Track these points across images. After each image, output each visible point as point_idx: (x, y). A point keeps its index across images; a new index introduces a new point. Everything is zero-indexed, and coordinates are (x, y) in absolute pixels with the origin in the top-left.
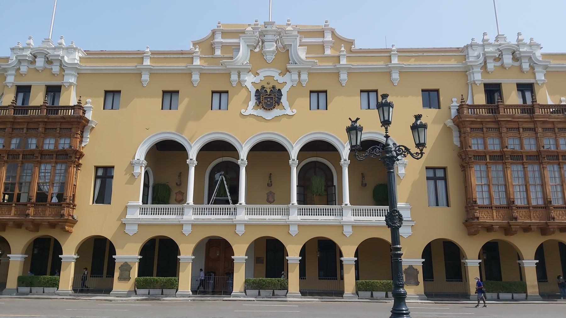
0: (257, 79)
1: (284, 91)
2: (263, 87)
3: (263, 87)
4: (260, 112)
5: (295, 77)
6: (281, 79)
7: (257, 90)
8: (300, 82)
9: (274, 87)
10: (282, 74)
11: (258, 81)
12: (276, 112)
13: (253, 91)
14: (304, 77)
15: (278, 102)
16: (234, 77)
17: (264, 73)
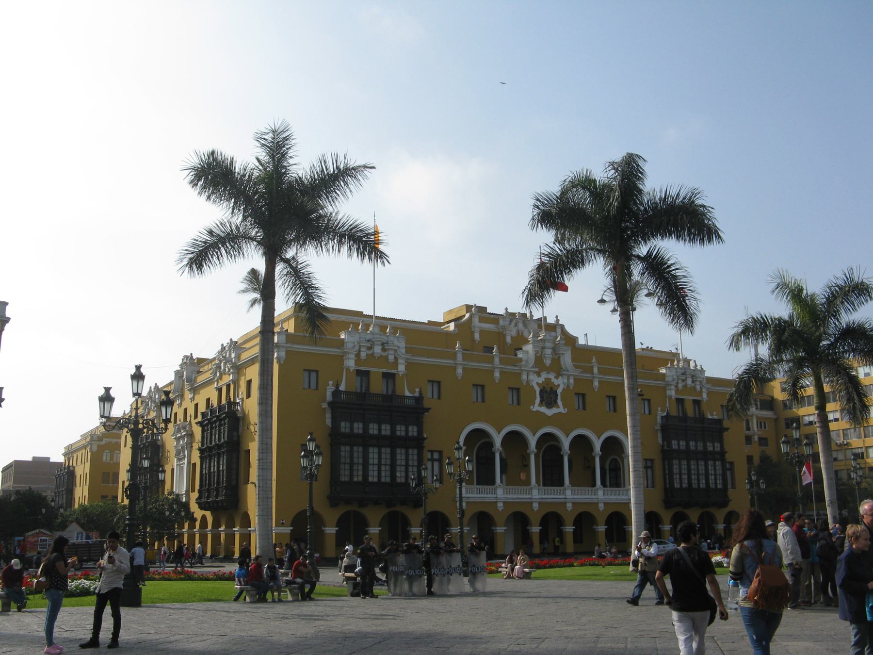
0: (541, 380)
1: (559, 391)
2: (544, 388)
3: (544, 388)
4: (544, 409)
5: (566, 381)
6: (556, 382)
7: (541, 391)
8: (568, 386)
9: (551, 388)
10: (557, 377)
11: (540, 382)
12: (554, 410)
13: (538, 390)
14: (572, 381)
15: (556, 402)
16: (524, 377)
17: (544, 375)
